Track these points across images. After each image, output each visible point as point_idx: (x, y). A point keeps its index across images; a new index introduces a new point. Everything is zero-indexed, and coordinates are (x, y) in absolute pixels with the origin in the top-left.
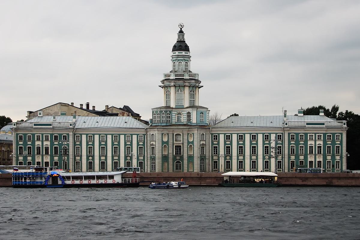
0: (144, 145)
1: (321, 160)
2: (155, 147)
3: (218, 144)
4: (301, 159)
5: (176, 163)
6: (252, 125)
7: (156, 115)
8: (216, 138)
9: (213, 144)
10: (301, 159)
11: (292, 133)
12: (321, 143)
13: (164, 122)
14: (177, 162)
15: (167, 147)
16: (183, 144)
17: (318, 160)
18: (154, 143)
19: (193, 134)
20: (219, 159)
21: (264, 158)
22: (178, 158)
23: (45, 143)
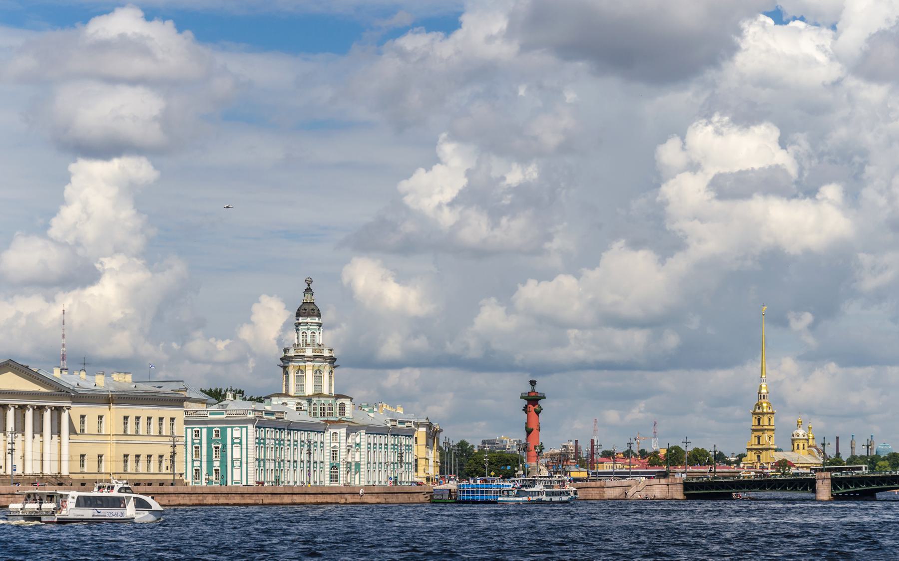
0: (323, 447)
2: (339, 450)
18: (338, 445)
19: (360, 433)
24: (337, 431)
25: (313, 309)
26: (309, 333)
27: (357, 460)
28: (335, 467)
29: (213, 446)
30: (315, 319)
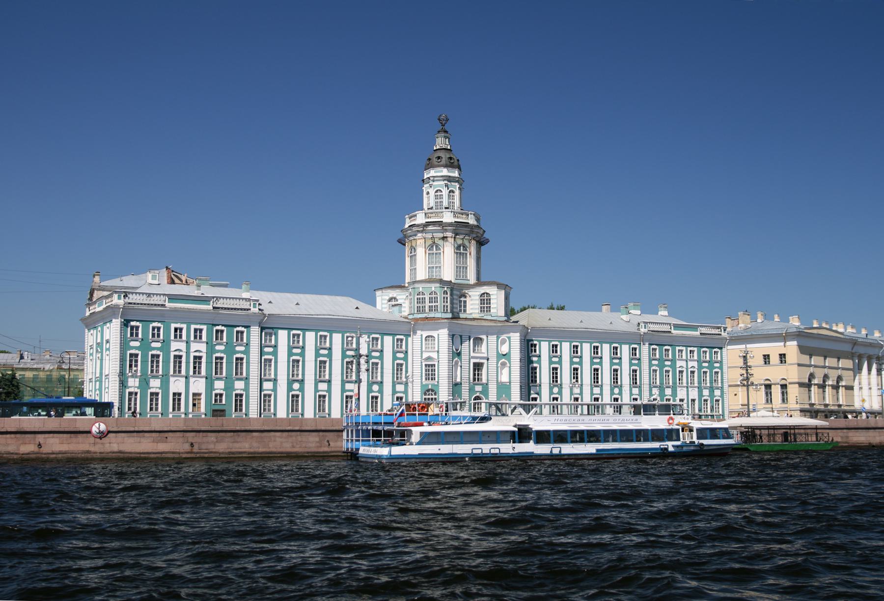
0: (406, 359)
1: (696, 397)
2: (436, 364)
5: (474, 399)
6: (583, 325)
7: (423, 294)
13: (447, 310)
14: (476, 399)
15: (460, 363)
16: (488, 360)
17: (690, 398)
18: (434, 355)
19: (509, 338)
23: (194, 346)
24: (434, 333)
25: (439, 158)
26: (432, 192)
27: (504, 378)
28: (432, 391)
29: (97, 356)
30: (442, 171)
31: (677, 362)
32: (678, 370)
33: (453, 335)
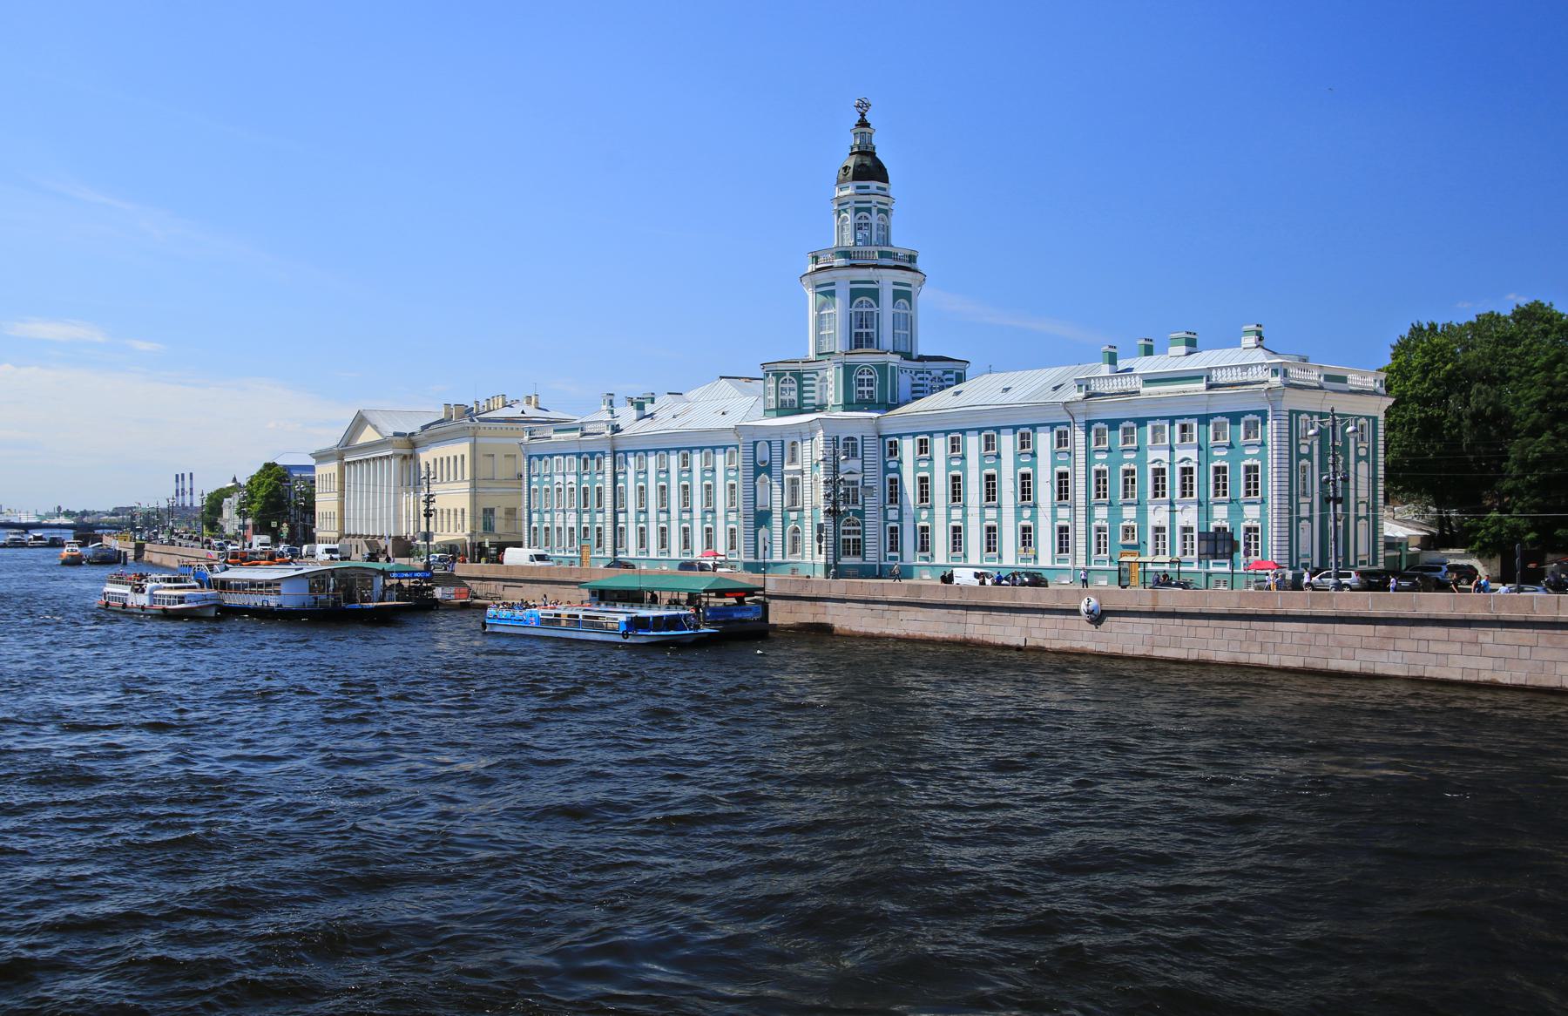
3: (898, 470)
4: (1125, 520)
8: (894, 449)
9: (887, 470)
10: (1125, 520)
11: (1097, 421)
12: (1193, 454)
16: (802, 473)
20: (900, 519)
21: (1018, 517)
22: (793, 515)
31: (1149, 451)
32: (1150, 468)
33: (755, 443)
